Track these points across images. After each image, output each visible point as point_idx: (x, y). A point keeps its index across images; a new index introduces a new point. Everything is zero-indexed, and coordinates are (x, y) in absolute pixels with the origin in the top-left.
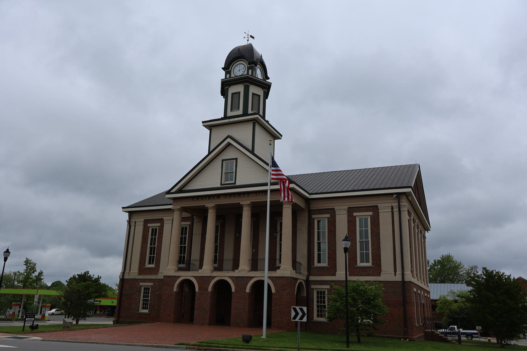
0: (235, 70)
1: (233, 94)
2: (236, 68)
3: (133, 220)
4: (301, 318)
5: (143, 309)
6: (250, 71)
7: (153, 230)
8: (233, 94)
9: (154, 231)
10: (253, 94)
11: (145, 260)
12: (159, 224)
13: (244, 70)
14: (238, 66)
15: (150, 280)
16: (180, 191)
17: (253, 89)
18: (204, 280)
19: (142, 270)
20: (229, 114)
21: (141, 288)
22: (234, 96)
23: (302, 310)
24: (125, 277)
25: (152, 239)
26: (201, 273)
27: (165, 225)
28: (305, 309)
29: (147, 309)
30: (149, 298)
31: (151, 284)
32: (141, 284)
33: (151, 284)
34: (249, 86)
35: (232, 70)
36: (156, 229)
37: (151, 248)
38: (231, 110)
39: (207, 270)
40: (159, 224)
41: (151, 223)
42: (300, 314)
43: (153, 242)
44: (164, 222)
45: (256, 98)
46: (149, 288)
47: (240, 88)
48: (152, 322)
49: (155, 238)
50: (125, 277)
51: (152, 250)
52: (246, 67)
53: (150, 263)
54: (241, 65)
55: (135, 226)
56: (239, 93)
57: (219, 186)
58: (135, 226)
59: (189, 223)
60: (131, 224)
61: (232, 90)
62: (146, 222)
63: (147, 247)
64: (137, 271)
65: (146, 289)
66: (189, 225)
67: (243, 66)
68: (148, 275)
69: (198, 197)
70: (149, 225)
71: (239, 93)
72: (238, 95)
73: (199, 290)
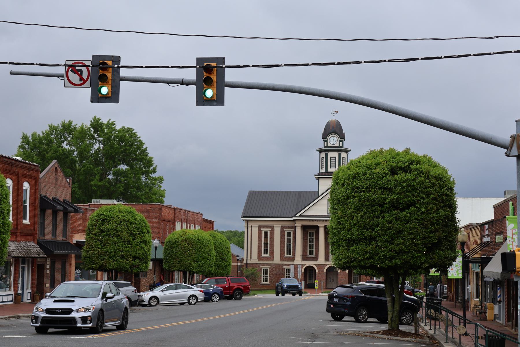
0: (330, 140)
1: (331, 157)
2: (331, 138)
3: (250, 226)
4: (407, 285)
5: (264, 281)
6: (341, 143)
7: (265, 232)
8: (331, 157)
9: (266, 234)
10: (343, 158)
11: (262, 252)
12: (270, 229)
13: (337, 141)
14: (332, 137)
15: (268, 264)
16: (300, 216)
17: (344, 155)
18: (321, 267)
19: (260, 258)
20: (329, 170)
21: (261, 269)
22: (332, 158)
23: (407, 282)
24: (248, 262)
25: (265, 238)
26: (318, 262)
27: (275, 230)
28: (409, 282)
29: (267, 281)
30: (268, 275)
31: (270, 267)
32: (261, 267)
33: (270, 267)
34: (341, 153)
35: (328, 140)
36: (267, 232)
37: (265, 244)
38: (331, 168)
39: (321, 260)
40: (270, 229)
41: (263, 228)
42: (407, 284)
43: (266, 240)
44: (274, 228)
45: (344, 159)
46: (267, 270)
47: (336, 154)
48: (267, 290)
49: (267, 238)
50: (248, 262)
51: (266, 246)
52: (338, 141)
53: (264, 254)
54: (334, 137)
55: (251, 229)
56: (335, 157)
57: (327, 214)
58: (251, 229)
59: (293, 230)
60: (248, 228)
61: (330, 154)
62: (260, 227)
63: (262, 243)
64: (257, 259)
65: (265, 270)
66: (293, 231)
67: (336, 138)
68: (266, 261)
69: (313, 220)
70: (262, 229)
71: (335, 157)
72: (334, 158)
73: (318, 271)
